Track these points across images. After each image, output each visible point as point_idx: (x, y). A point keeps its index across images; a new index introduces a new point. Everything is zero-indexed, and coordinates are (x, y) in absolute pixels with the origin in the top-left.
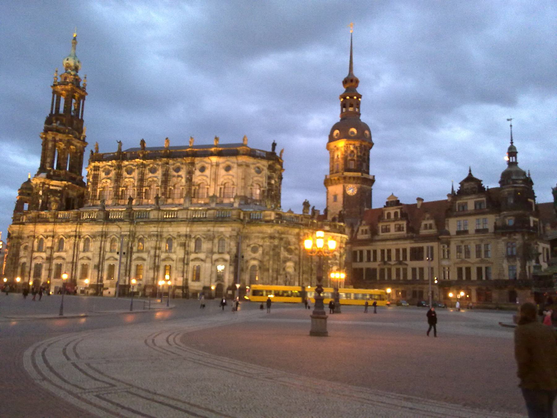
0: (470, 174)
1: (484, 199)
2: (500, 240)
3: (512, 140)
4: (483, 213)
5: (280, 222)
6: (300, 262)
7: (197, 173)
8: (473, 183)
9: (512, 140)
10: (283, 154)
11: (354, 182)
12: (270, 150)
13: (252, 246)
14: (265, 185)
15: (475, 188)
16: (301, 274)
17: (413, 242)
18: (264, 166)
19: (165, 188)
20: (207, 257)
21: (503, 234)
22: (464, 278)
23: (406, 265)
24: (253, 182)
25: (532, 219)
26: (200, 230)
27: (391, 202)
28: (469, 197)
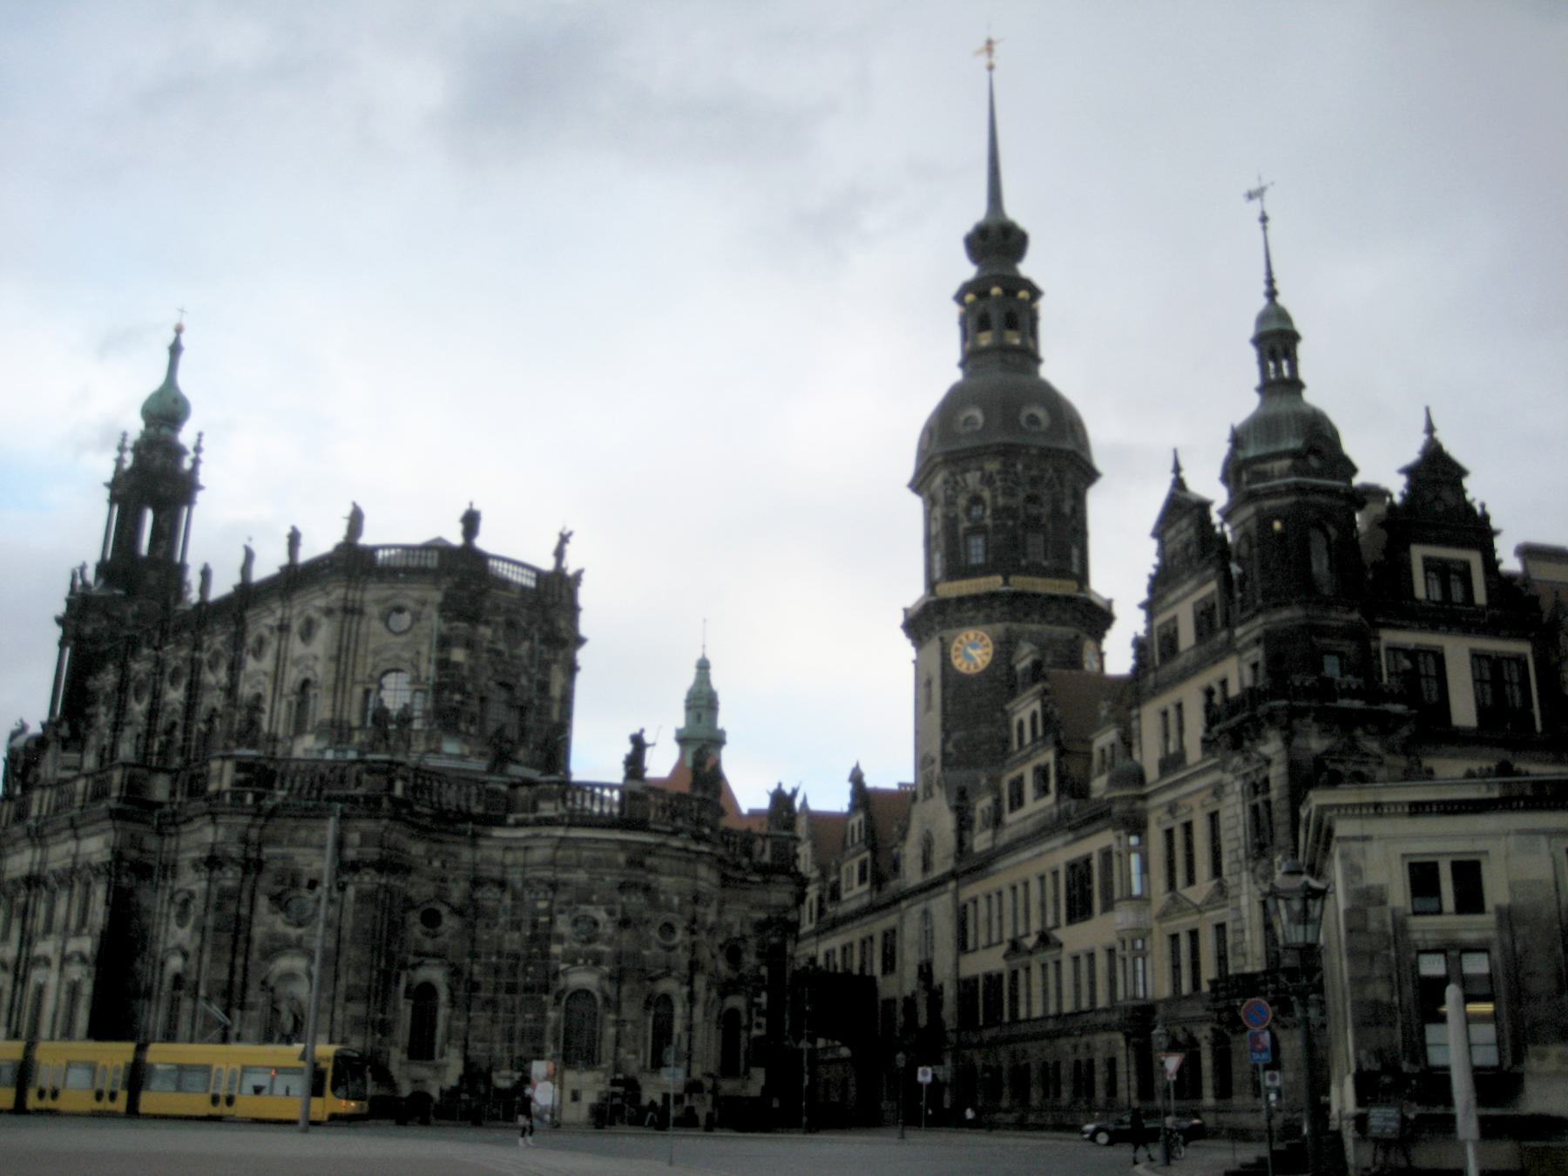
0: (1179, 484)
1: (1212, 586)
2: (1228, 777)
3: (1270, 281)
4: (1215, 657)
5: (249, 799)
6: (338, 953)
7: (251, 664)
8: (1184, 523)
9: (1270, 281)
10: (568, 548)
11: (981, 616)
12: (455, 538)
13: (179, 898)
14: (429, 670)
15: (1187, 546)
16: (340, 1000)
17: (1070, 836)
18: (423, 603)
19: (187, 730)
20: (55, 951)
21: (1237, 746)
22: (1186, 987)
23: (1060, 945)
24: (375, 667)
25: (1458, 651)
26: (59, 854)
27: (1026, 669)
28: (1179, 592)
